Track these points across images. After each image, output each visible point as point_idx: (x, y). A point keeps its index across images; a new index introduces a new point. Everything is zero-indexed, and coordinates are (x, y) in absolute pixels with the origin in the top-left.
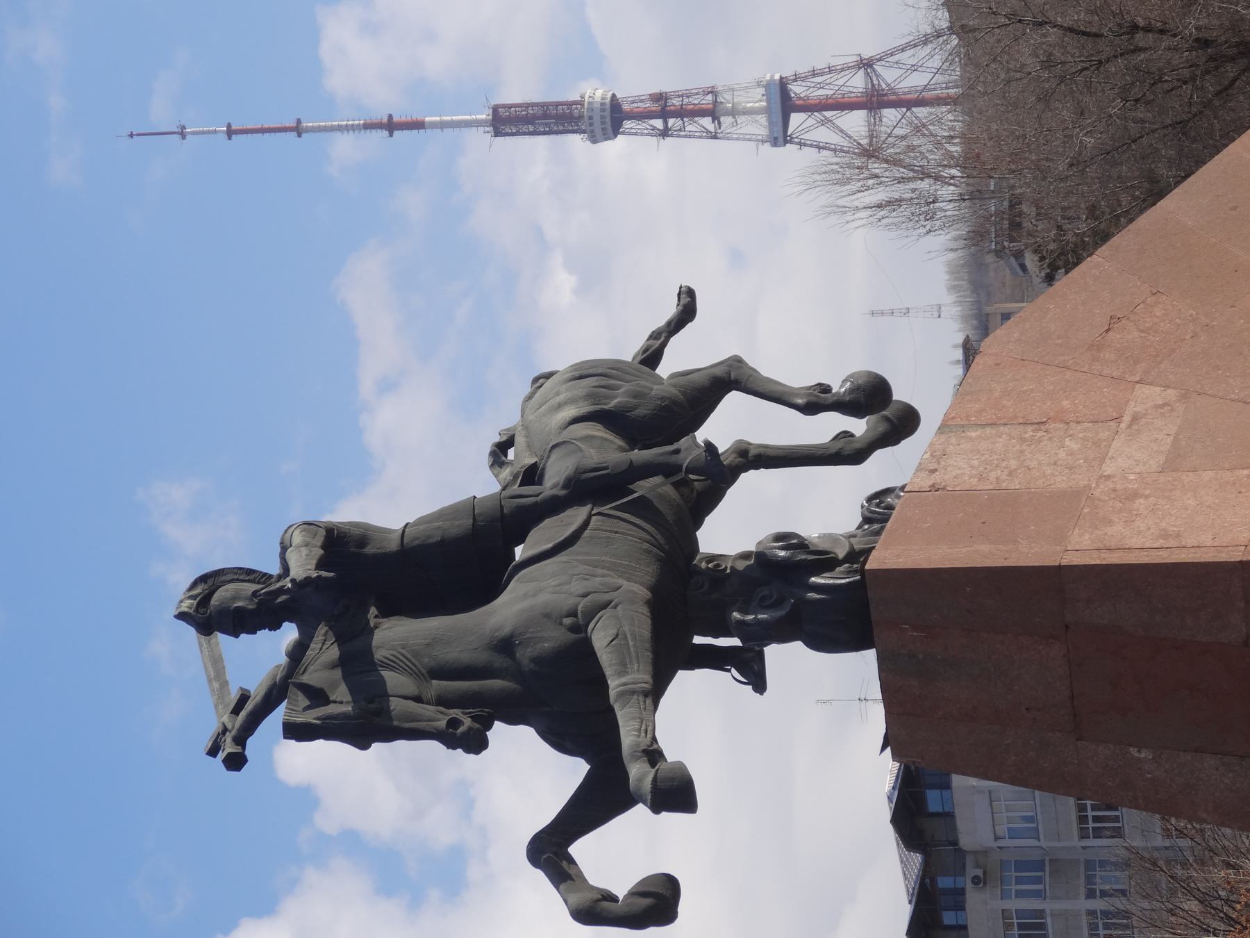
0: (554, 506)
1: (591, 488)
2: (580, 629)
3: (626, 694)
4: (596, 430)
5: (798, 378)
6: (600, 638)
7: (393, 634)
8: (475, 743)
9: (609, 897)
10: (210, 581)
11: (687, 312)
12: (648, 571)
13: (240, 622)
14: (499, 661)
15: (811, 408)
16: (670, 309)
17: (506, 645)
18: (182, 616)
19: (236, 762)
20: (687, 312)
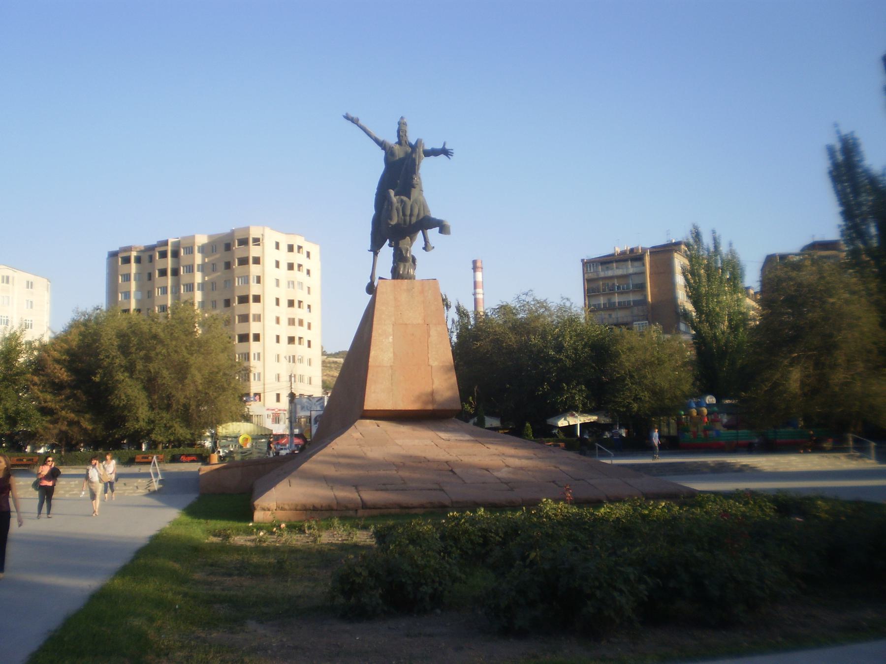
18: (402, 118)
19: (354, 121)
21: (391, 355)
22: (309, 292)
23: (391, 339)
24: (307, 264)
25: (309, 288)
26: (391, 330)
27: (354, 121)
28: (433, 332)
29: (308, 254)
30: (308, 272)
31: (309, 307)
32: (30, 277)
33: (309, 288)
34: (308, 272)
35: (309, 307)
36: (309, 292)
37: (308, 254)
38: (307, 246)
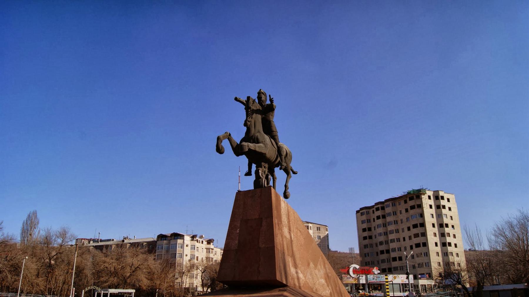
0: (277, 144)
1: (279, 150)
2: (262, 142)
3: (255, 146)
4: (285, 153)
5: (289, 185)
6: (261, 144)
7: (258, 118)
8: (245, 125)
9: (221, 142)
10: (265, 94)
11: (294, 173)
12: (268, 155)
13: (259, 98)
14: (257, 131)
15: (286, 186)
16: (295, 170)
17: (259, 132)
19: (236, 99)
20: (294, 173)
21: (237, 242)
22: (452, 219)
23: (238, 231)
24: (447, 205)
25: (451, 217)
26: (239, 225)
27: (236, 99)
28: (264, 223)
29: (448, 200)
30: (450, 209)
31: (453, 226)
32: (318, 226)
33: (451, 217)
34: (450, 209)
35: (453, 226)
36: (452, 219)
37: (448, 200)
38: (446, 196)
